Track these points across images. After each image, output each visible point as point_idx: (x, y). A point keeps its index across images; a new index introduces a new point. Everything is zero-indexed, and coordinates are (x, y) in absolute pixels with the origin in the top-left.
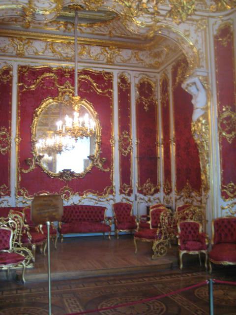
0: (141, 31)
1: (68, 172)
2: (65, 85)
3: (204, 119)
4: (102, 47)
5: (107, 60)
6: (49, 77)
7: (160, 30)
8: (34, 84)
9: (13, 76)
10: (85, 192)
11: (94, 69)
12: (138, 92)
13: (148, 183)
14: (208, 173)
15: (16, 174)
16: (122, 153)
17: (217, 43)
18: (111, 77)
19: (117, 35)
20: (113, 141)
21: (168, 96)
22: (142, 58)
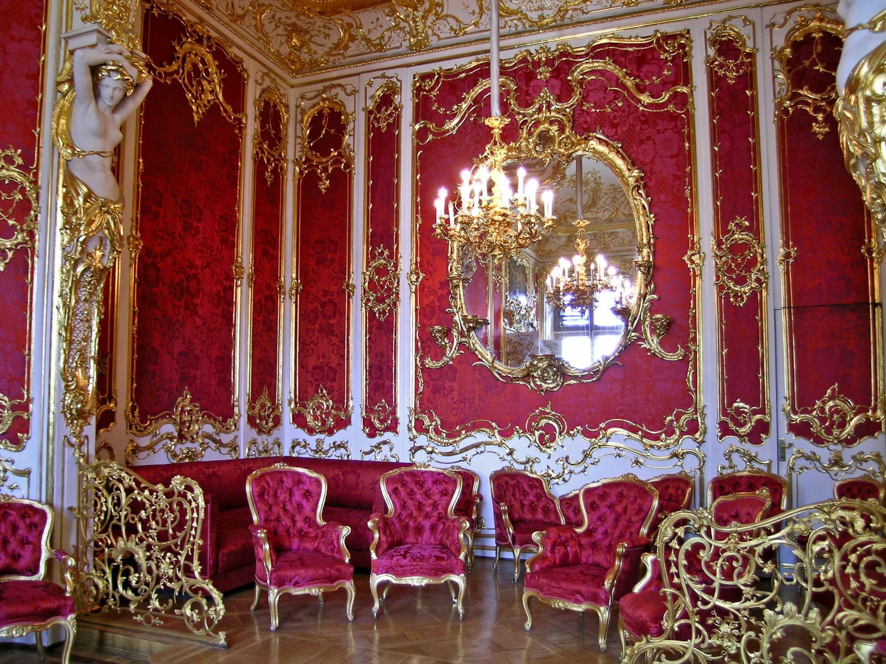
9: (402, 108)
10: (602, 425)
12: (781, 76)
13: (831, 398)
16: (727, 295)
18: (682, 46)
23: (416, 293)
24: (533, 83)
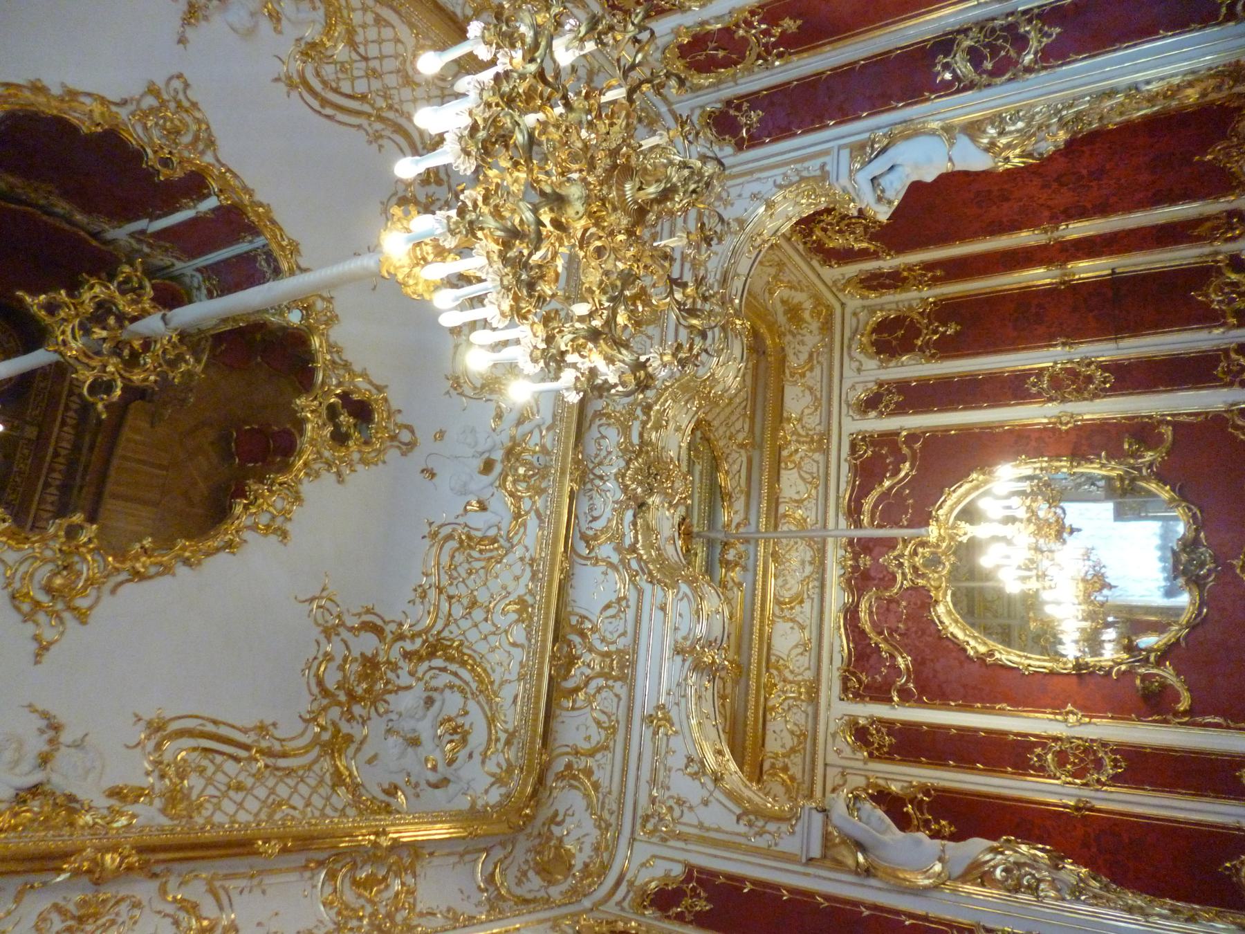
0: (737, 352)
1: (1184, 557)
2: (892, 568)
3: (984, 132)
4: (783, 465)
5: (814, 451)
6: (871, 613)
7: (732, 301)
8: (892, 657)
9: (872, 717)
11: (843, 486)
13: (1207, 296)
14: (1176, 81)
15: (1197, 731)
16: (1102, 390)
17: (755, 141)
18: (863, 439)
19: (746, 427)
20: (1064, 419)
21: (910, 268)
22: (804, 357)
23: (1091, 717)
24: (873, 574)
